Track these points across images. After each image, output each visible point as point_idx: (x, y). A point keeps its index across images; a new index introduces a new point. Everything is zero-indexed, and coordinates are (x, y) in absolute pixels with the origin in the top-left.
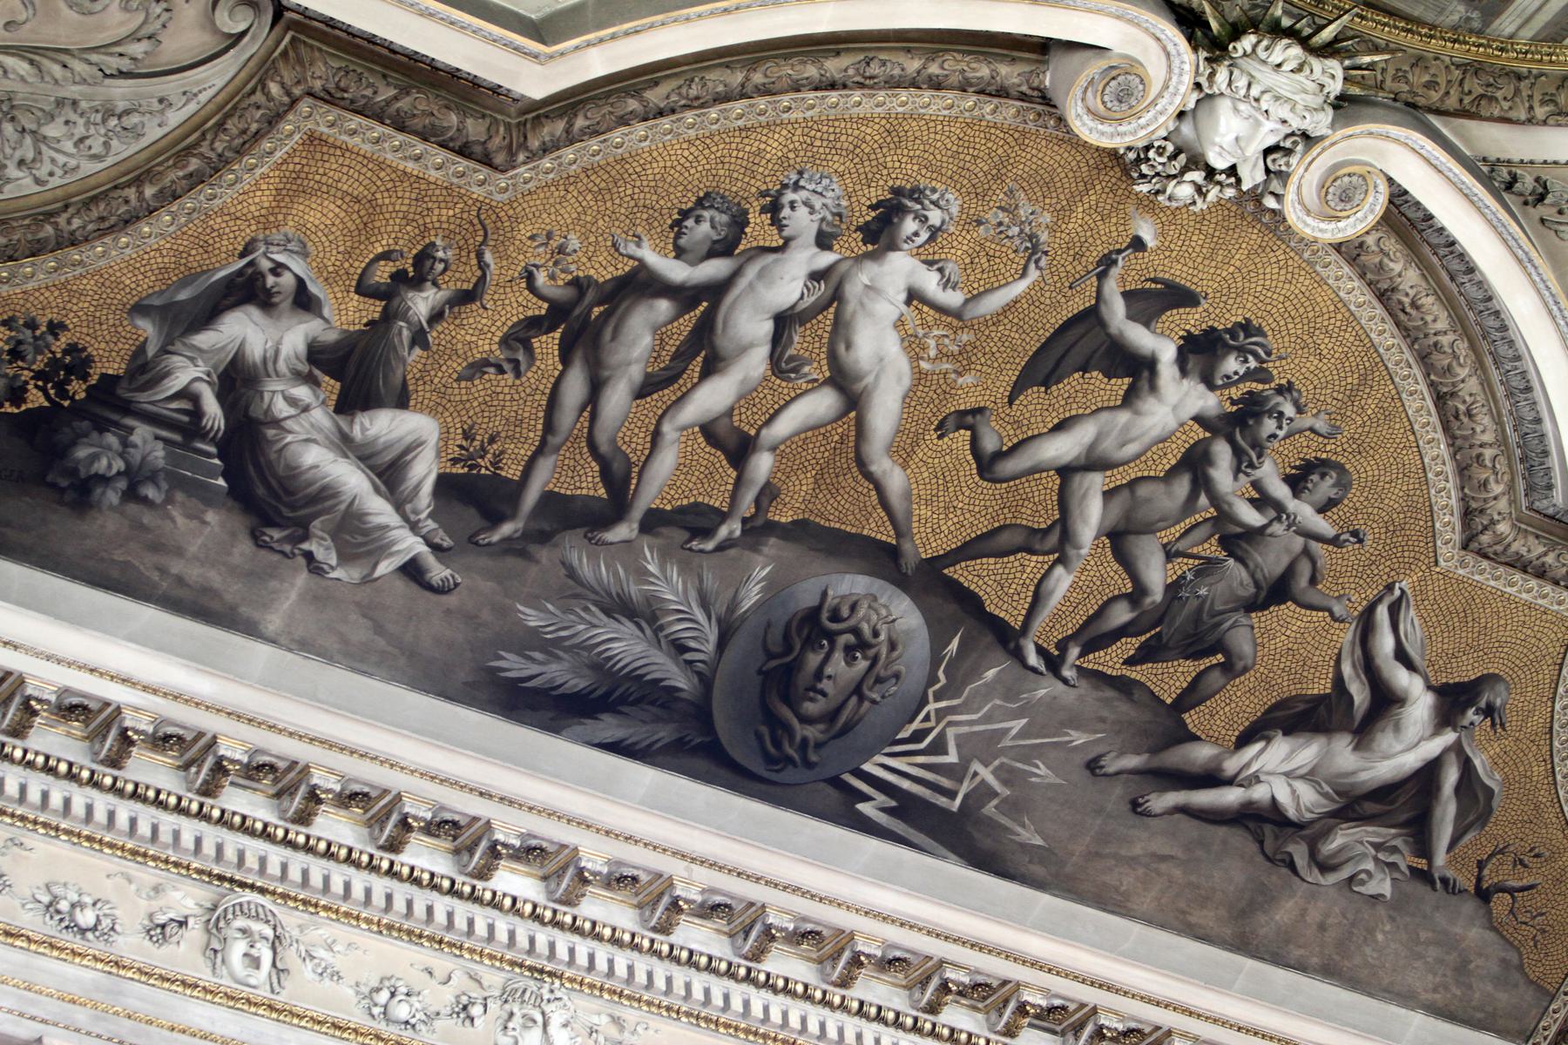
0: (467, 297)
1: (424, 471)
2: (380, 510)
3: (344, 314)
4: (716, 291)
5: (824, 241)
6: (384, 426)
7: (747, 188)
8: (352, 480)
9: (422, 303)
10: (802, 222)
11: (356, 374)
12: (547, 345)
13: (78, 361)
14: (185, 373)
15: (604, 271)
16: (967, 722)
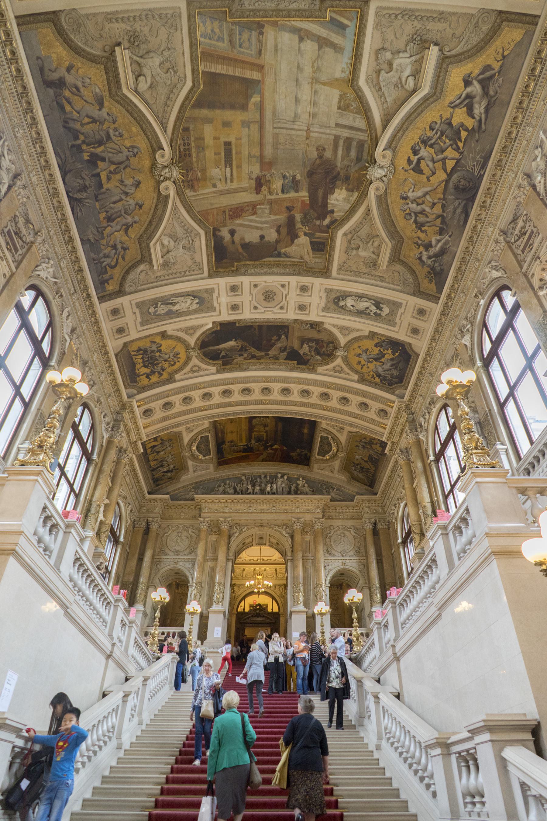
0: (419, 238)
1: (438, 238)
2: (443, 241)
3: (422, 249)
4: (416, 214)
5: (408, 204)
6: (434, 243)
7: (403, 215)
8: (440, 245)
9: (420, 242)
10: (406, 207)
11: (428, 246)
12: (423, 229)
13: (429, 272)
14: (429, 262)
15: (414, 225)
16: (471, 163)
